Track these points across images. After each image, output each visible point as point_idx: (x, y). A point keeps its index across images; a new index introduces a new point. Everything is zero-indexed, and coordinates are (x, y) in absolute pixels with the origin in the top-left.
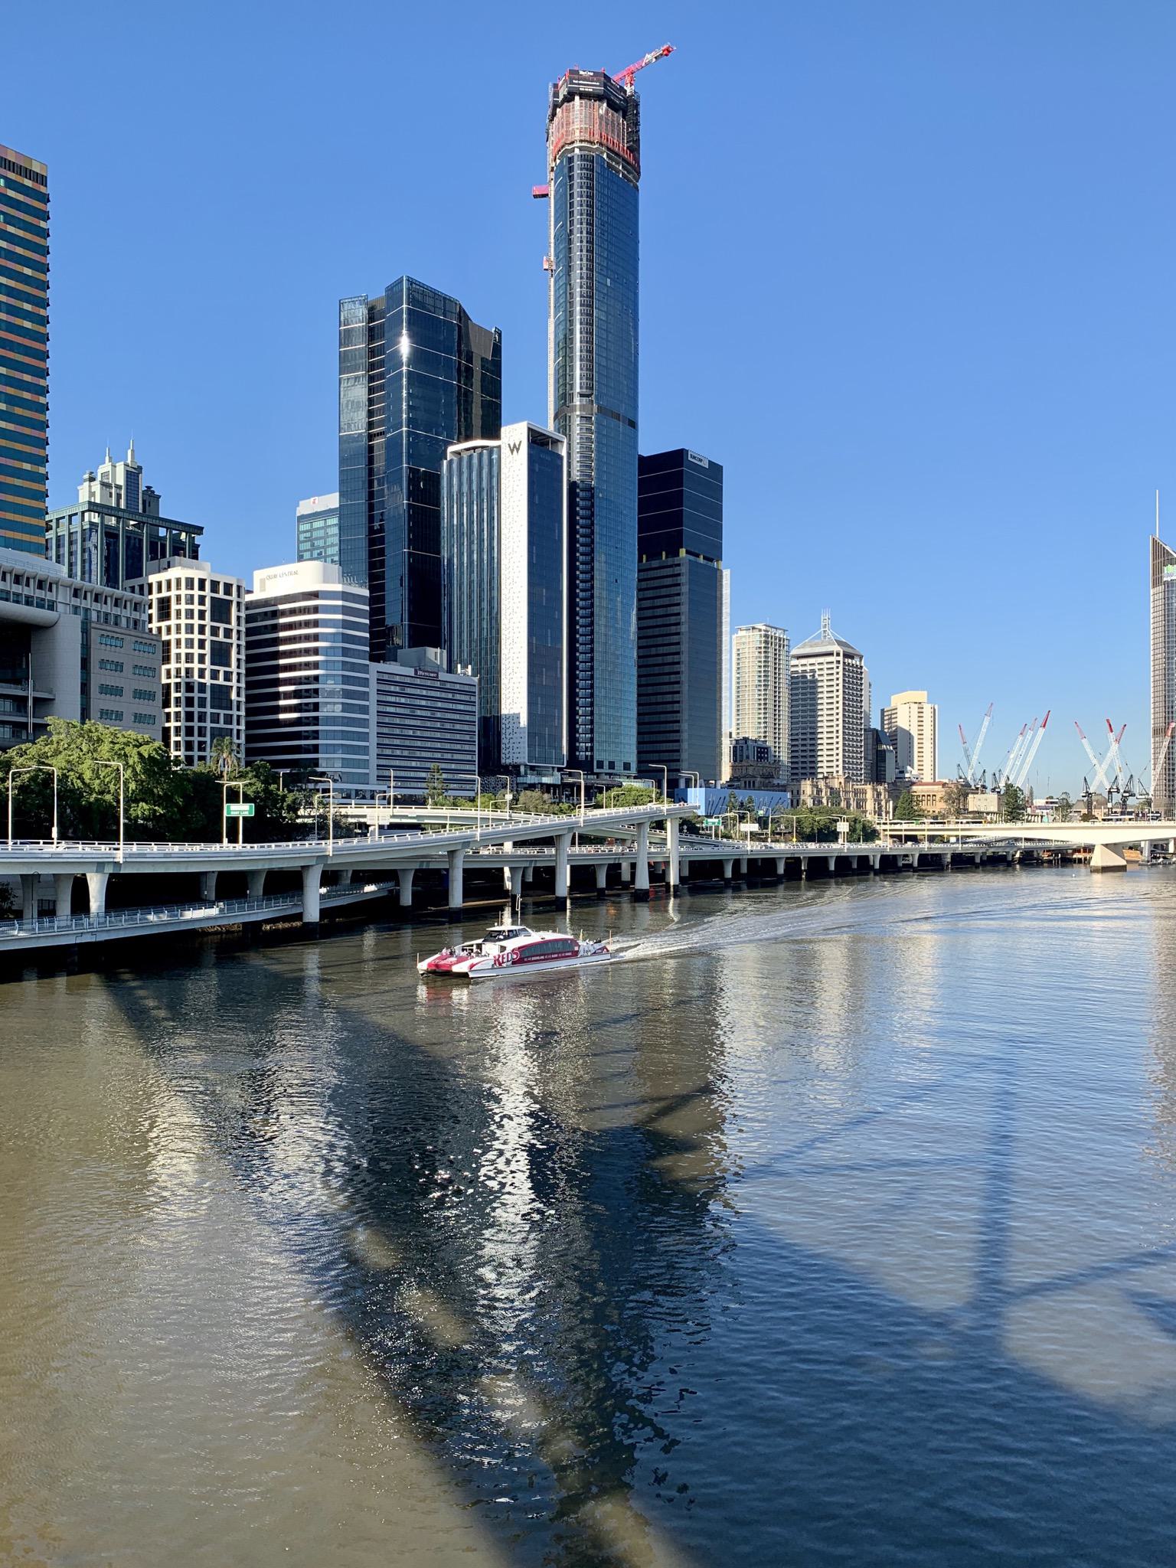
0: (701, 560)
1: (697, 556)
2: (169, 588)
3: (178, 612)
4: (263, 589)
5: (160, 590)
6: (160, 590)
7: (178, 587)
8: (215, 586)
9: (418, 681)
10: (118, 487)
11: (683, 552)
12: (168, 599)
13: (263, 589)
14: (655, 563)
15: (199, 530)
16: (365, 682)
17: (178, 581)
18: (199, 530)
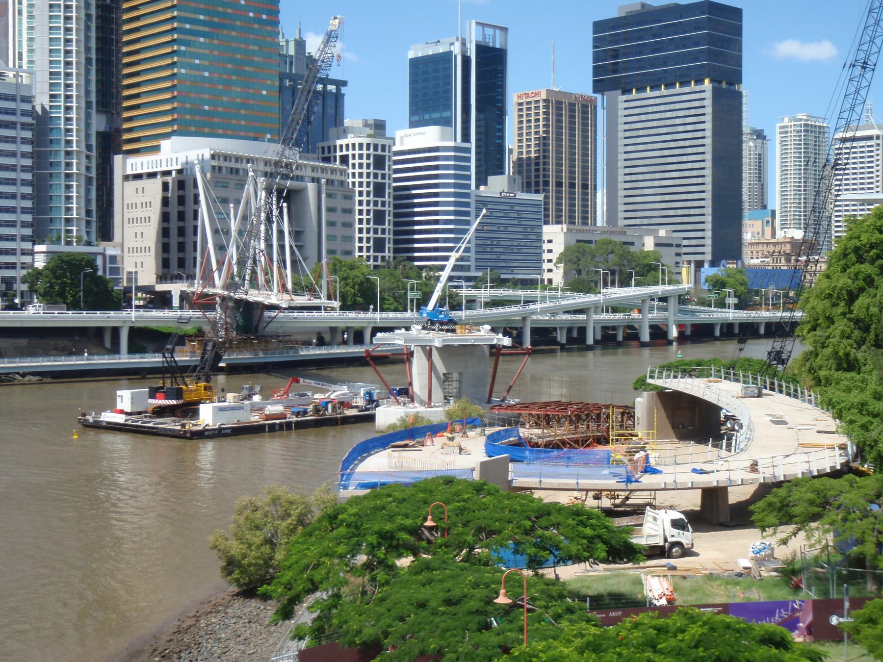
0: (724, 85)
1: (720, 82)
2: (348, 150)
3: (354, 165)
4: (402, 144)
5: (341, 150)
6: (341, 150)
7: (354, 149)
8: (376, 147)
9: (503, 200)
10: (291, 57)
11: (707, 81)
12: (347, 156)
13: (402, 144)
14: (686, 89)
15: (344, 83)
16: (467, 205)
17: (354, 145)
18: (344, 83)
